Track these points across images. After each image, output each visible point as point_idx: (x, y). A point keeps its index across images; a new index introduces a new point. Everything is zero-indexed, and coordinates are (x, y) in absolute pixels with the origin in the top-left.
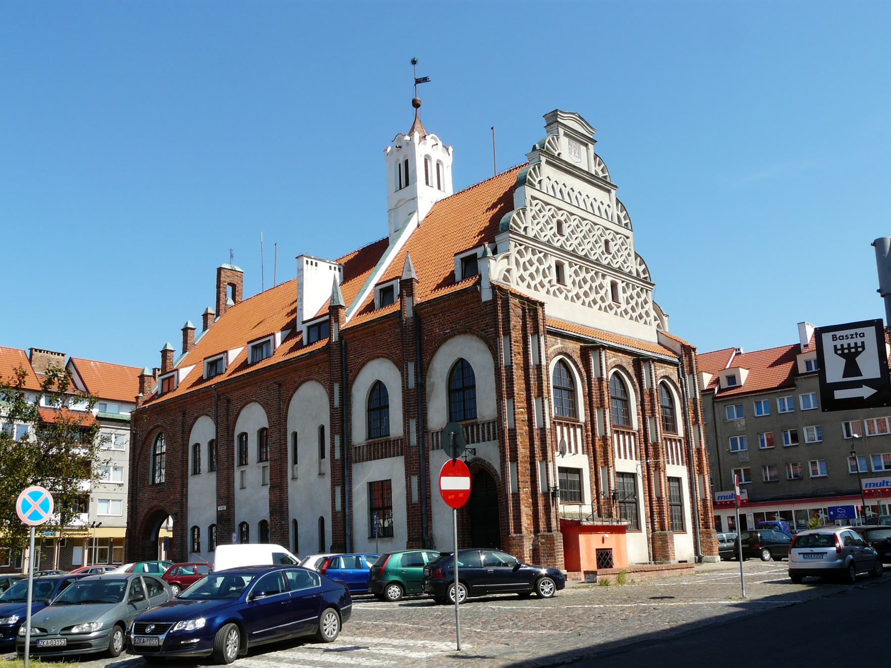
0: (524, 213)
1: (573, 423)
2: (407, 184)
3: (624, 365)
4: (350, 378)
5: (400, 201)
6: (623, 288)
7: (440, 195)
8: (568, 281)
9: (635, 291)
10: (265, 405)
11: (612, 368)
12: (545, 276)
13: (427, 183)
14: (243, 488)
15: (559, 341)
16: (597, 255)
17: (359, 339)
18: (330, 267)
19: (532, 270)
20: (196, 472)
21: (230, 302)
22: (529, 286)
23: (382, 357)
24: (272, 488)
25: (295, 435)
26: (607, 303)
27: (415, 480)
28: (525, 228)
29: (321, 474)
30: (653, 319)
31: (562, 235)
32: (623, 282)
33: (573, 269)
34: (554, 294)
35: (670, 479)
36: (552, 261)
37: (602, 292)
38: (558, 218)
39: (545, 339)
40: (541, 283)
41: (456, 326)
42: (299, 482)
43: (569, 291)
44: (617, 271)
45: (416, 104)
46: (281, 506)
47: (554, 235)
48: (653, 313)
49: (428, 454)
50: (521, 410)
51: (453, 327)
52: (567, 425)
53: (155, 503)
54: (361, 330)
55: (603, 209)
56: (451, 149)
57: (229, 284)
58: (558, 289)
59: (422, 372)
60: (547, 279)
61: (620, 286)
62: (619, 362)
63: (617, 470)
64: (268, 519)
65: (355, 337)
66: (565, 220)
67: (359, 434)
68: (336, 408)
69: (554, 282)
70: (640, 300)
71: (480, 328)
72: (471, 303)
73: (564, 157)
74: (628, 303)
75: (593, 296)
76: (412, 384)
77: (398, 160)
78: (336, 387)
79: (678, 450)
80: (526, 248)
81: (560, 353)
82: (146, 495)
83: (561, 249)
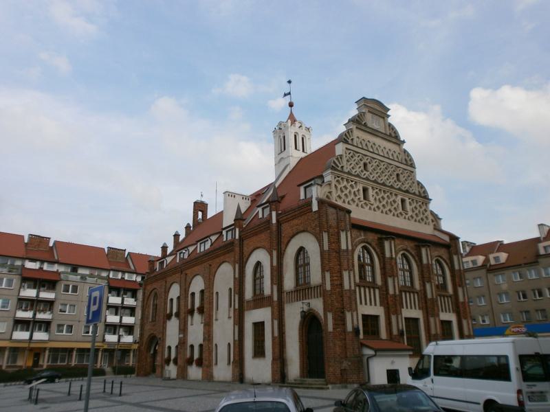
0: (341, 158)
1: (373, 285)
2: (285, 149)
3: (409, 249)
4: (245, 260)
6: (410, 202)
8: (372, 199)
10: (203, 277)
11: (400, 251)
13: (296, 148)
14: (192, 325)
15: (362, 234)
19: (347, 192)
22: (344, 202)
24: (205, 325)
25: (217, 293)
26: (398, 212)
27: (276, 322)
28: (342, 167)
29: (229, 317)
30: (431, 221)
31: (367, 171)
34: (362, 207)
35: (443, 322)
36: (360, 187)
37: (395, 205)
38: (364, 161)
39: (351, 233)
40: (352, 200)
43: (372, 205)
44: (405, 192)
45: (291, 105)
46: (209, 336)
47: (362, 171)
48: (430, 217)
52: (364, 287)
53: (152, 332)
55: (395, 156)
59: (281, 256)
61: (408, 201)
62: (405, 247)
66: (369, 163)
67: (248, 294)
69: (362, 199)
70: (421, 210)
73: (369, 125)
74: (413, 211)
76: (275, 263)
78: (237, 266)
79: (449, 303)
80: (342, 179)
83: (367, 179)
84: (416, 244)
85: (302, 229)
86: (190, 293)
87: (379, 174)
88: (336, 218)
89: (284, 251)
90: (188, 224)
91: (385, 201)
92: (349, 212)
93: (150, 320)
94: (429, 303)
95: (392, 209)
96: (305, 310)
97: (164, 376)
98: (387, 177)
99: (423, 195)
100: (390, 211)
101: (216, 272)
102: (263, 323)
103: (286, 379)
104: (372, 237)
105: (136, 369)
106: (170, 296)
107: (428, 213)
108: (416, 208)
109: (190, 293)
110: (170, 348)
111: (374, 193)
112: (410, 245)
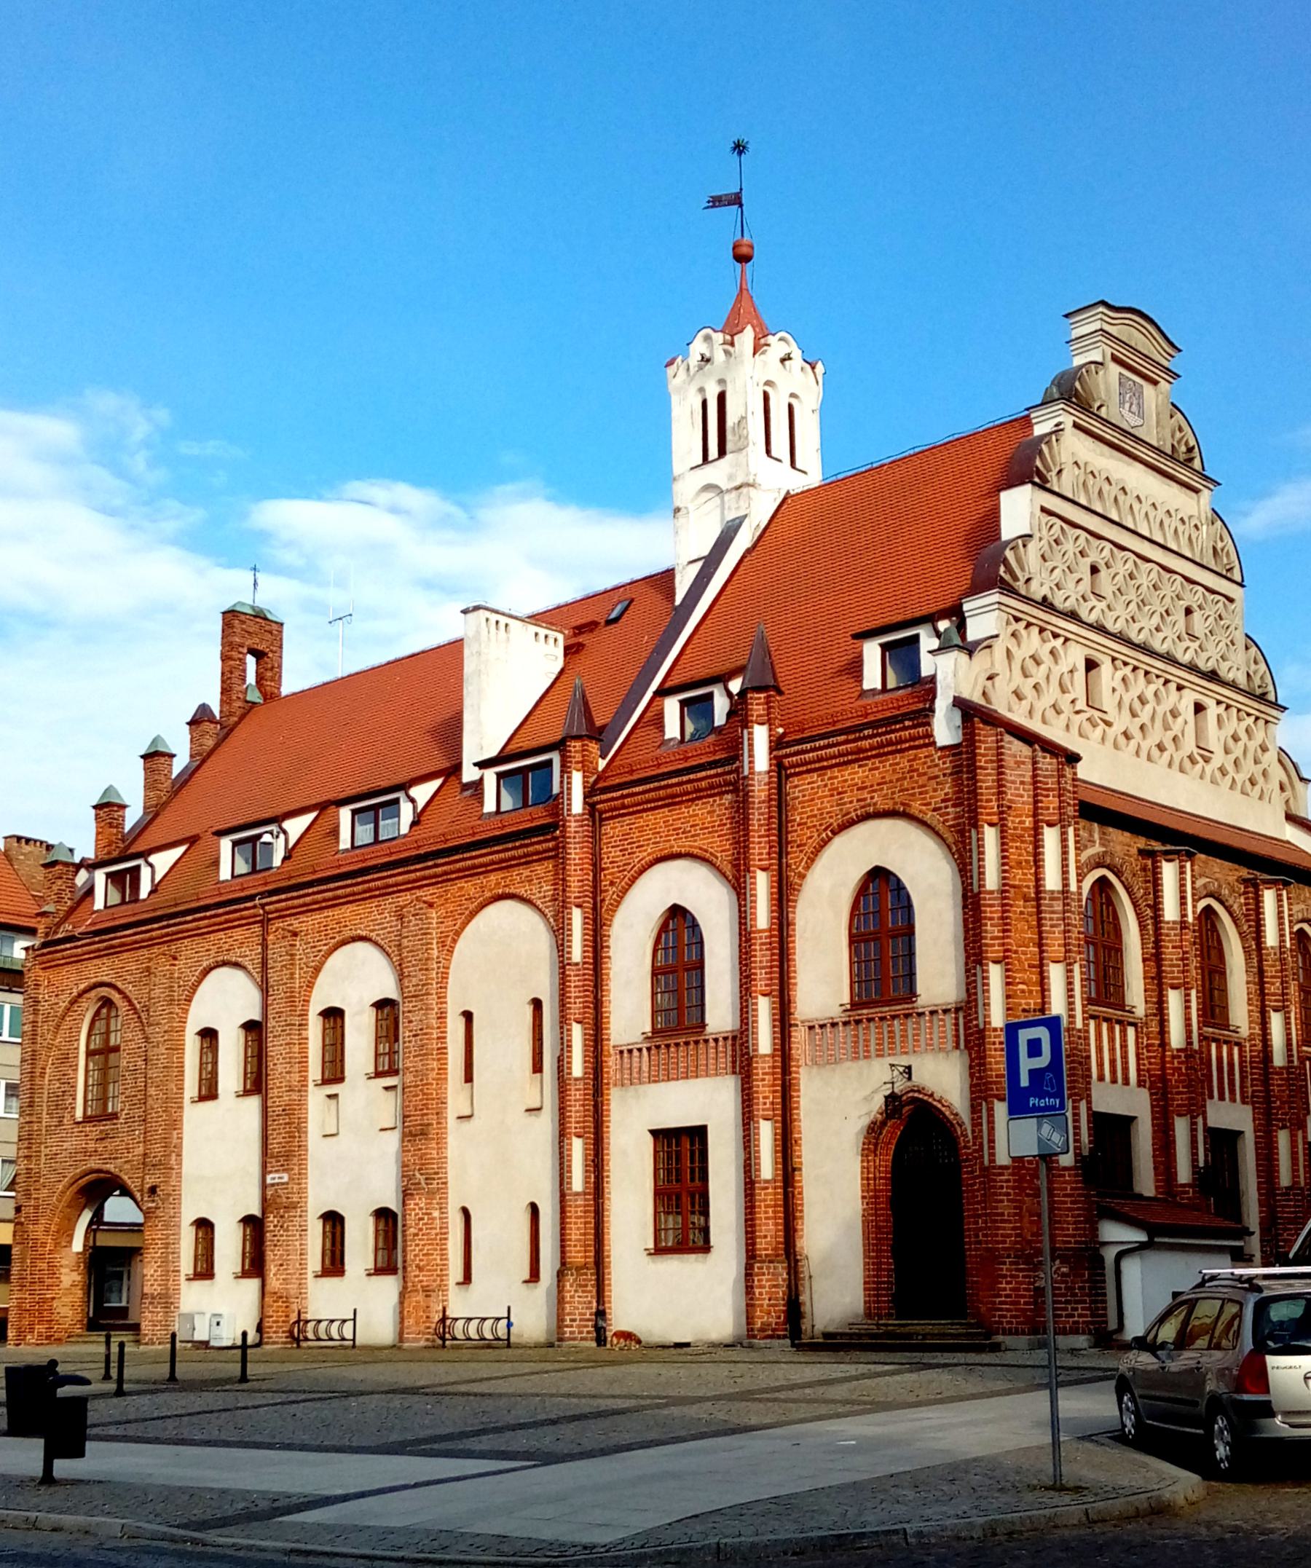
2: (722, 452)
6: (1219, 716)
7: (798, 483)
9: (1244, 725)
12: (1064, 690)
13: (768, 452)
16: (1169, 641)
18: (536, 634)
20: (209, 1092)
21: (255, 696)
31: (1099, 597)
32: (1219, 703)
33: (1119, 674)
36: (1075, 656)
37: (1177, 726)
41: (872, 798)
48: (1277, 774)
49: (797, 1073)
50: (1021, 987)
51: (865, 799)
53: (94, 1163)
56: (820, 368)
57: (253, 652)
58: (1088, 719)
60: (1069, 697)
63: (1211, 1124)
68: (577, 964)
69: (1081, 705)
70: (1253, 745)
71: (929, 804)
72: (911, 748)
74: (1227, 751)
75: (1156, 735)
78: (577, 916)
81: (1099, 865)
82: (66, 1145)
84: (1244, 872)
85: (888, 805)
86: (316, 1007)
87: (1133, 606)
88: (1028, 779)
89: (802, 877)
90: (204, 709)
91: (1149, 708)
92: (1073, 758)
93: (79, 1114)
94: (1276, 1080)
95: (1135, 731)
96: (896, 1090)
98: (1156, 619)
99: (1258, 692)
100: (1223, 771)
101: (458, 934)
102: (699, 1134)
103: (806, 1325)
104: (1124, 844)
105: (12, 1317)
106: (198, 1016)
107: (1270, 758)
108: (1236, 738)
109: (319, 1002)
110: (204, 1226)
111: (1117, 683)
112: (1225, 874)
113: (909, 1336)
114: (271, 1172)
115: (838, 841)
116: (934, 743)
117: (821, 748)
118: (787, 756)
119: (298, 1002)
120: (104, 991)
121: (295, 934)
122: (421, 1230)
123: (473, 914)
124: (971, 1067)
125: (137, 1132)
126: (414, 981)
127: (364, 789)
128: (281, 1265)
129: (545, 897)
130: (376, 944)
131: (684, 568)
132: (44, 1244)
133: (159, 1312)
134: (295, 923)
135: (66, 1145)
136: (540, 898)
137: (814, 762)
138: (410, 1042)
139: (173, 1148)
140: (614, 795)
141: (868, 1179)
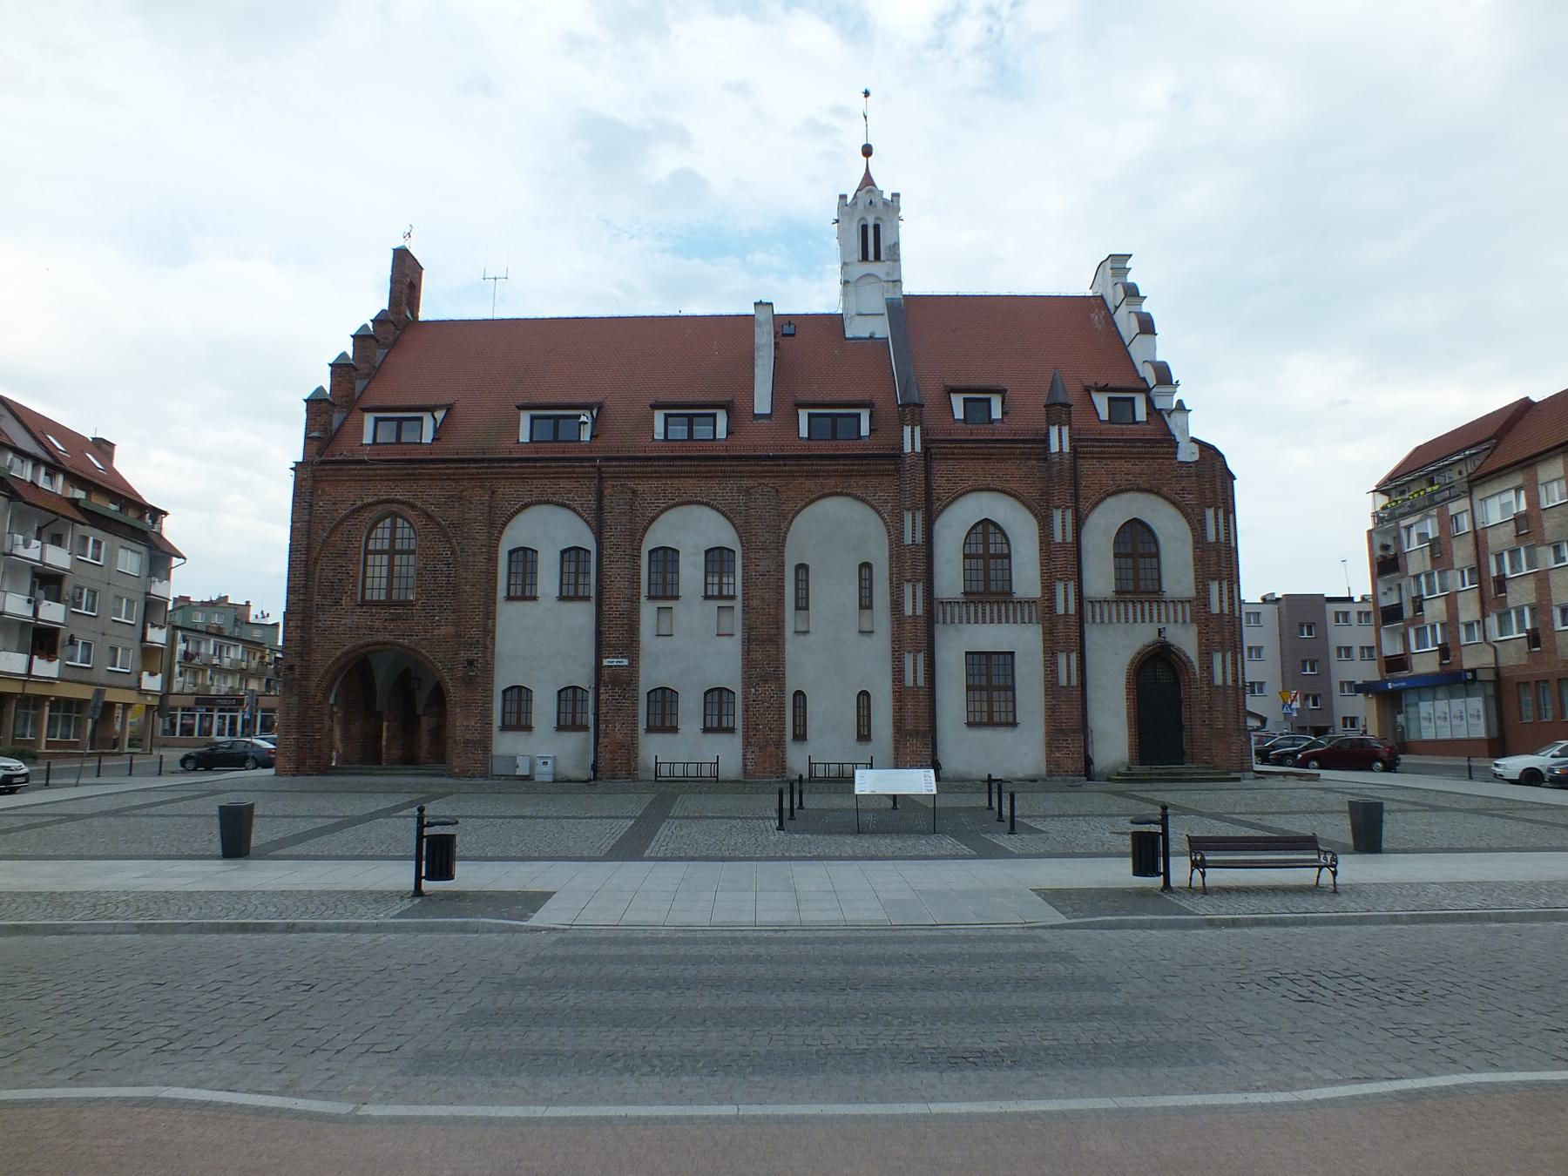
2: (877, 257)
5: (868, 275)
17: (958, 459)
23: (1003, 492)
24: (748, 642)
25: (802, 568)
42: (811, 638)
45: (867, 151)
51: (1131, 480)
54: (970, 448)
59: (1079, 524)
64: (737, 688)
65: (952, 454)
68: (918, 545)
72: (1160, 458)
77: (863, 218)
78: (919, 517)
82: (343, 621)
89: (1087, 516)
97: (498, 768)
101: (797, 513)
113: (1182, 774)
114: (608, 657)
115: (1110, 502)
116: (1176, 458)
117: (1106, 447)
118: (1081, 447)
119: (636, 538)
120: (394, 507)
121: (634, 492)
122: (772, 704)
123: (812, 501)
124: (1199, 633)
125: (437, 618)
126: (762, 539)
127: (566, 401)
128: (623, 723)
129: (879, 499)
130: (718, 510)
131: (851, 317)
132: (315, 696)
133: (479, 754)
134: (631, 484)
135: (343, 621)
136: (875, 500)
137: (1113, 453)
138: (758, 579)
139: (489, 632)
140: (949, 445)
141: (1129, 689)
